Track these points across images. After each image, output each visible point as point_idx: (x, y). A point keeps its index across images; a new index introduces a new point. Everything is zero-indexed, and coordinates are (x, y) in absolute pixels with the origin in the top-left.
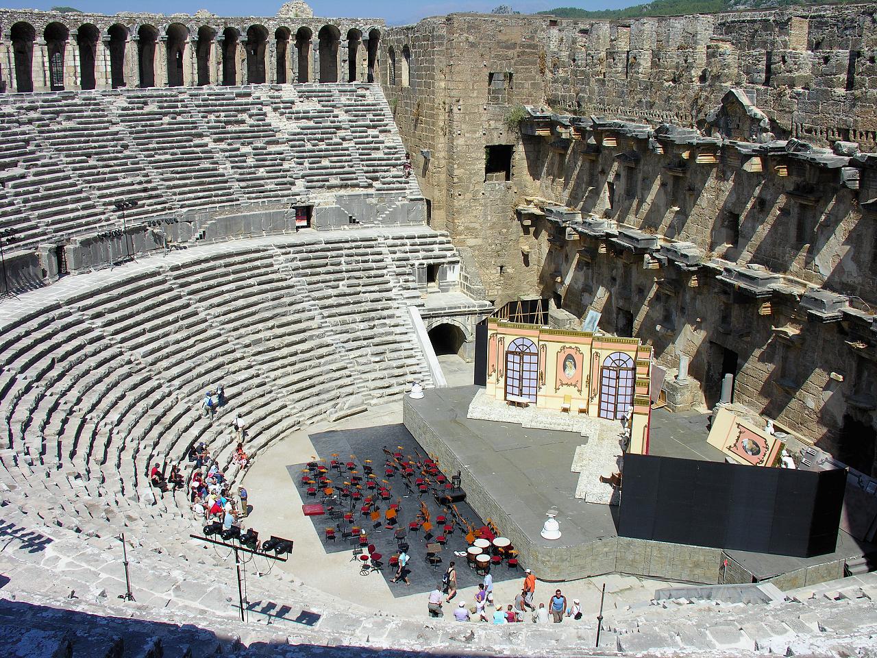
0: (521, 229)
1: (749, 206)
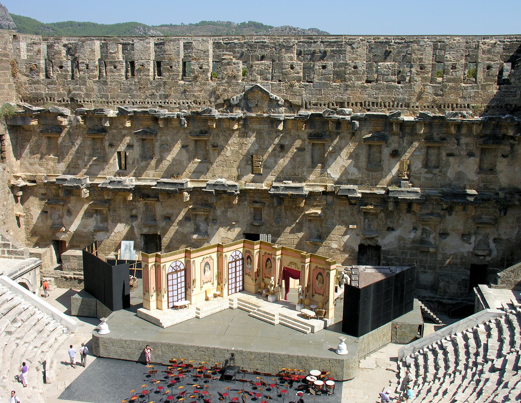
0: (14, 200)
1: (270, 150)
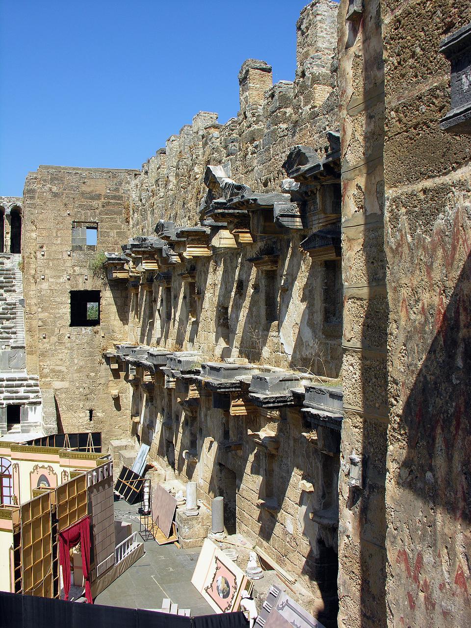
1: (233, 294)
